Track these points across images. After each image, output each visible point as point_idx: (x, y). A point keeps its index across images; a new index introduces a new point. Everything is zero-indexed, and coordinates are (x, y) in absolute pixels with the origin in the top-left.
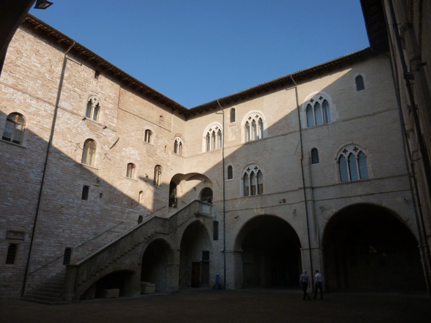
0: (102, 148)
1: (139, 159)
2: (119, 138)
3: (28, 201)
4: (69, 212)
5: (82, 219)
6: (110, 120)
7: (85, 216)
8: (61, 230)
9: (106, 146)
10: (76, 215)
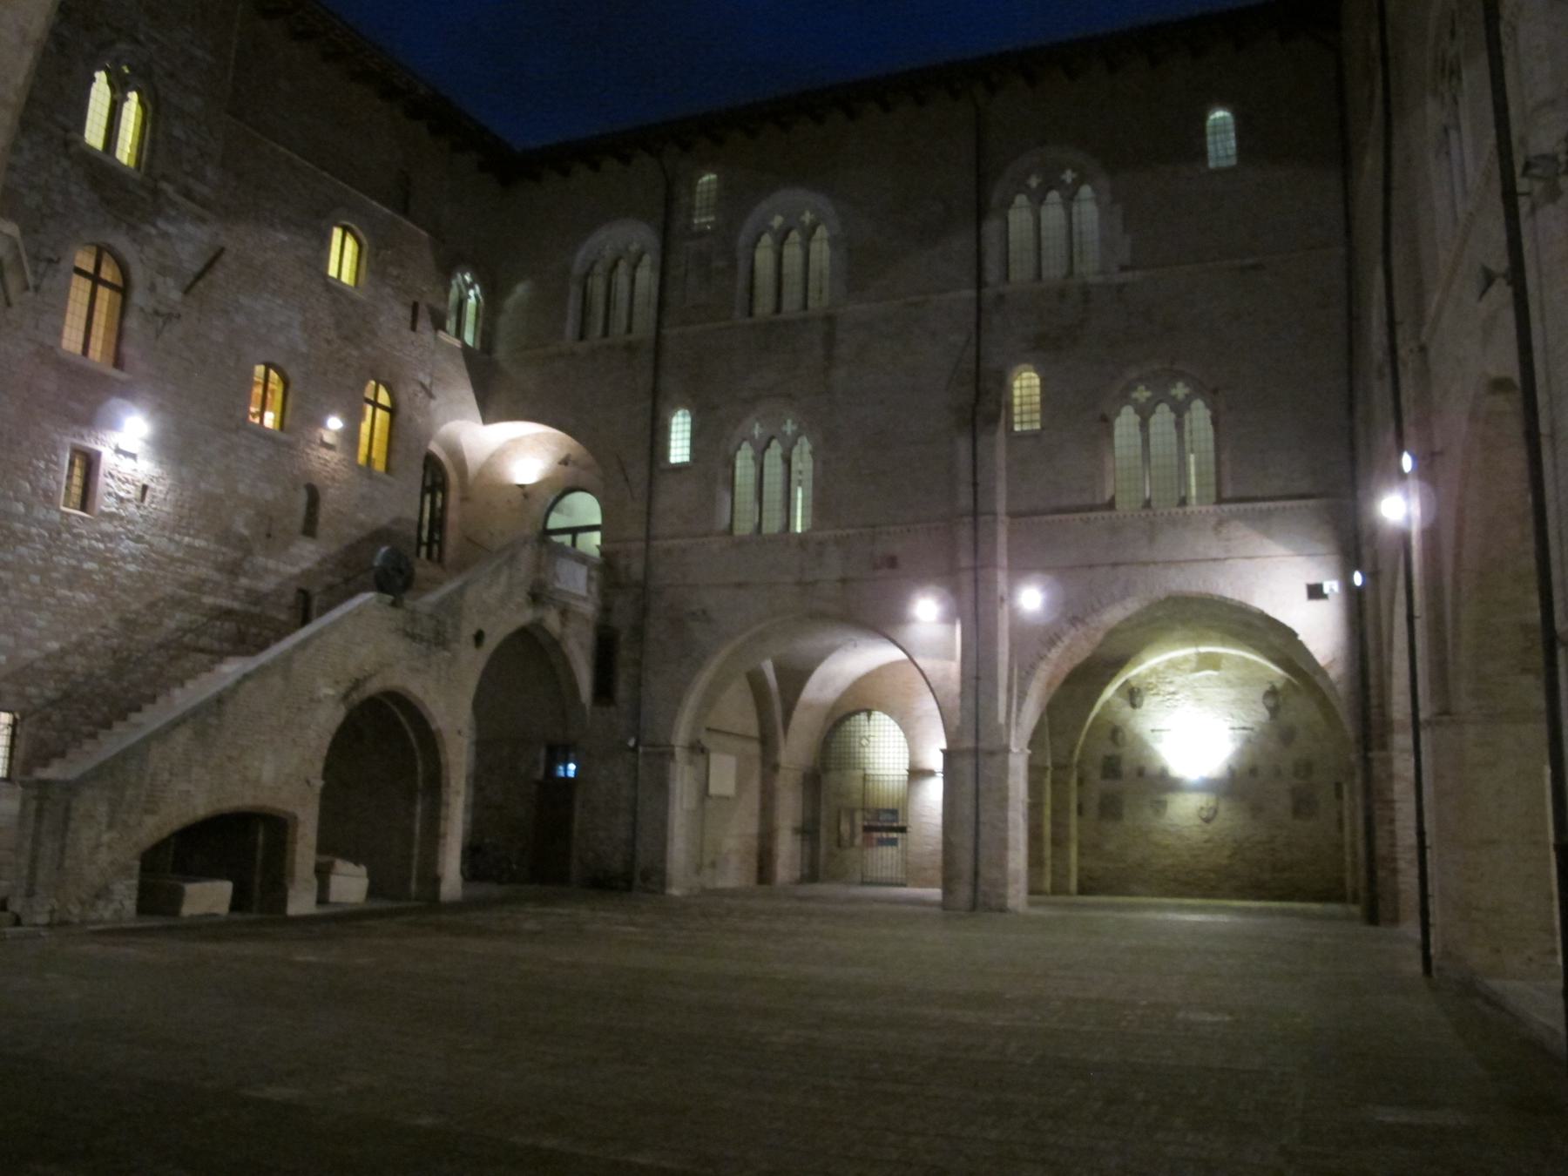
1: (304, 349)
2: (222, 250)
4: (10, 557)
6: (187, 168)
7: (75, 578)
9: (170, 282)
10: (37, 570)
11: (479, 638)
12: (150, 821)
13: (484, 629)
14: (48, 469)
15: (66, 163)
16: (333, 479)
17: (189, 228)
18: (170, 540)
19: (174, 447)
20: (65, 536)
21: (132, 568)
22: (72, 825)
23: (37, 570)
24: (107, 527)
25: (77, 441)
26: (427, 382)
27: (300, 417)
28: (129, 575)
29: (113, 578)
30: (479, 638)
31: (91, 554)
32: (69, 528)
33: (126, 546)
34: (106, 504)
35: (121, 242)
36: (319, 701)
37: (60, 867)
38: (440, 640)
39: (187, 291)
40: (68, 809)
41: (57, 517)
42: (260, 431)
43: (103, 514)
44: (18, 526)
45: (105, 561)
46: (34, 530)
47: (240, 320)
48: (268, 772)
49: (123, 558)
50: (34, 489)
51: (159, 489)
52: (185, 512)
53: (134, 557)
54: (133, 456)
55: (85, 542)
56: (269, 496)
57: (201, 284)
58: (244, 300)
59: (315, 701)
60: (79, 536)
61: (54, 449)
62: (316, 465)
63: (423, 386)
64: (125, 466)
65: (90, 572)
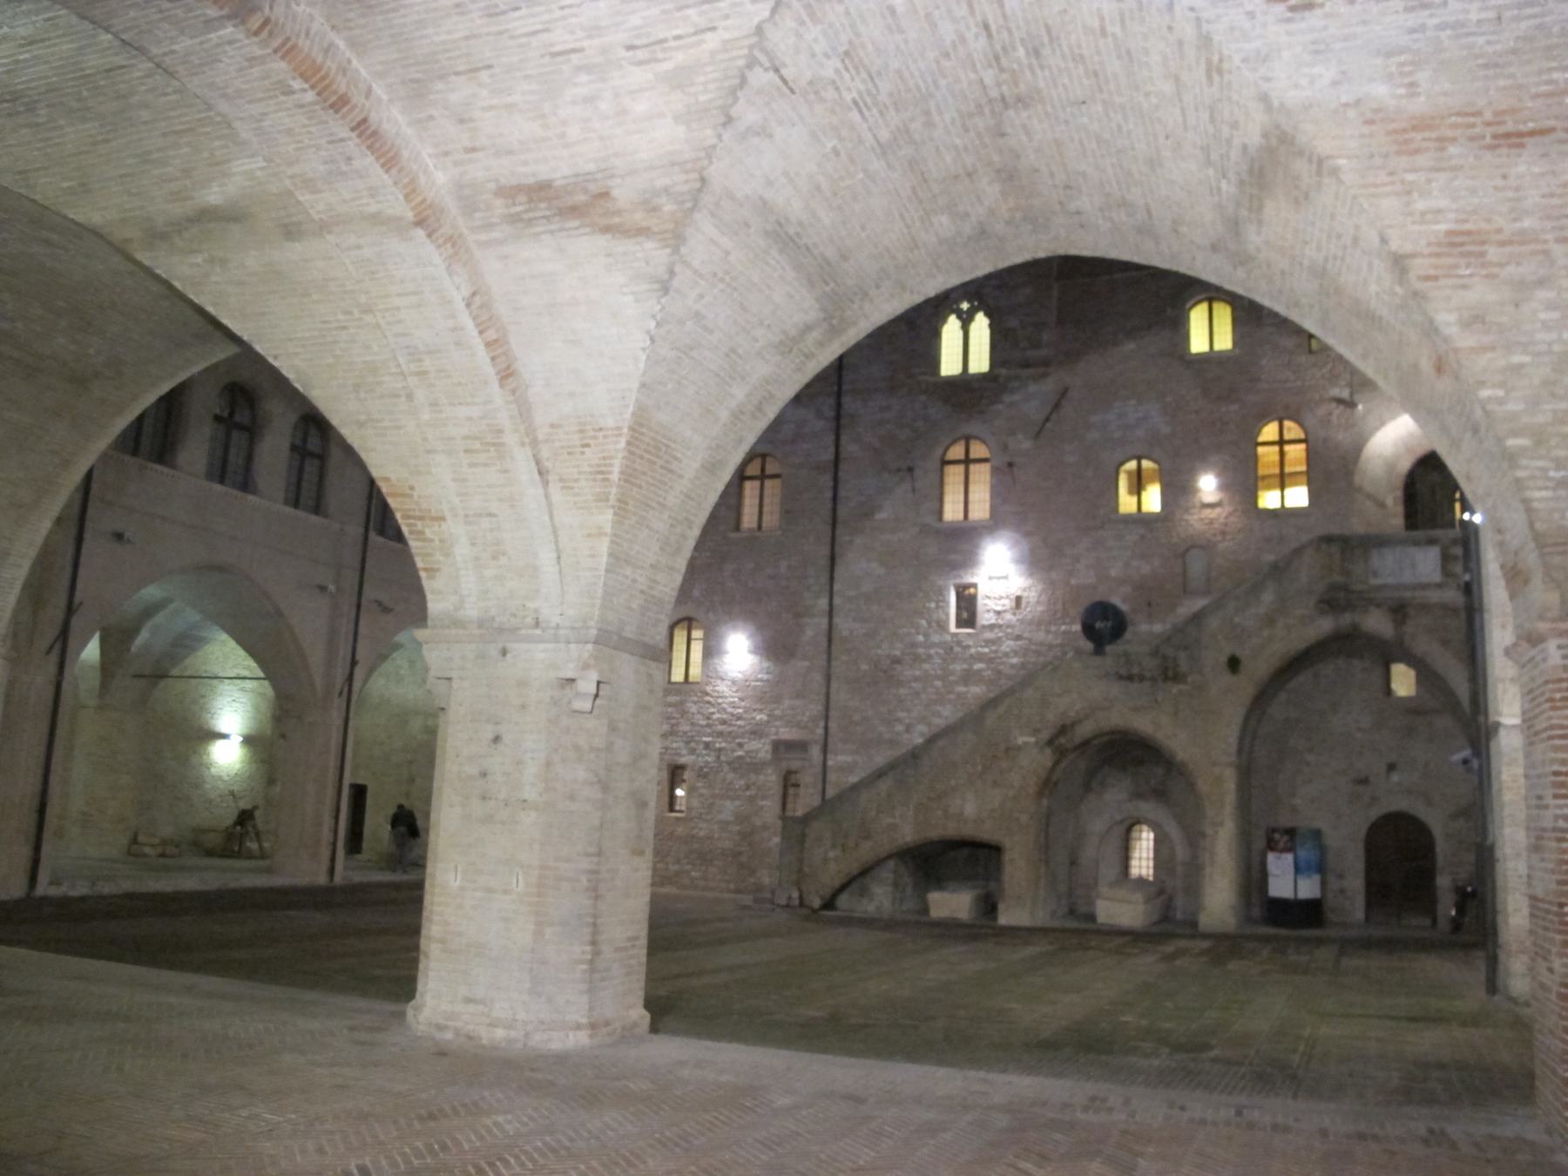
0: (1005, 447)
1: (1166, 430)
3: (806, 663)
4: (917, 673)
5: (962, 689)
7: (968, 677)
9: (1020, 436)
10: (937, 677)
11: (1234, 664)
12: (866, 846)
13: (1238, 653)
14: (938, 607)
15: (923, 398)
17: (1032, 388)
18: (1048, 632)
19: (1037, 561)
20: (957, 649)
21: (1015, 660)
22: (807, 845)
23: (937, 677)
24: (989, 635)
25: (958, 581)
26: (1345, 394)
27: (1178, 489)
28: (1013, 666)
29: (999, 672)
30: (1234, 664)
31: (980, 658)
32: (959, 643)
33: (1008, 645)
34: (985, 618)
35: (973, 428)
36: (1019, 748)
37: (800, 871)
38: (1170, 674)
40: (804, 835)
41: (948, 638)
42: (1141, 520)
43: (984, 627)
44: (921, 651)
45: (990, 661)
46: (932, 651)
47: (1094, 435)
48: (970, 809)
49: (1006, 655)
50: (929, 623)
51: (1032, 596)
52: (1059, 606)
53: (1016, 653)
54: (1006, 578)
55: (973, 651)
56: (1146, 569)
57: (1049, 425)
59: (1011, 751)
60: (968, 647)
62: (1199, 526)
63: (1340, 401)
65: (980, 671)
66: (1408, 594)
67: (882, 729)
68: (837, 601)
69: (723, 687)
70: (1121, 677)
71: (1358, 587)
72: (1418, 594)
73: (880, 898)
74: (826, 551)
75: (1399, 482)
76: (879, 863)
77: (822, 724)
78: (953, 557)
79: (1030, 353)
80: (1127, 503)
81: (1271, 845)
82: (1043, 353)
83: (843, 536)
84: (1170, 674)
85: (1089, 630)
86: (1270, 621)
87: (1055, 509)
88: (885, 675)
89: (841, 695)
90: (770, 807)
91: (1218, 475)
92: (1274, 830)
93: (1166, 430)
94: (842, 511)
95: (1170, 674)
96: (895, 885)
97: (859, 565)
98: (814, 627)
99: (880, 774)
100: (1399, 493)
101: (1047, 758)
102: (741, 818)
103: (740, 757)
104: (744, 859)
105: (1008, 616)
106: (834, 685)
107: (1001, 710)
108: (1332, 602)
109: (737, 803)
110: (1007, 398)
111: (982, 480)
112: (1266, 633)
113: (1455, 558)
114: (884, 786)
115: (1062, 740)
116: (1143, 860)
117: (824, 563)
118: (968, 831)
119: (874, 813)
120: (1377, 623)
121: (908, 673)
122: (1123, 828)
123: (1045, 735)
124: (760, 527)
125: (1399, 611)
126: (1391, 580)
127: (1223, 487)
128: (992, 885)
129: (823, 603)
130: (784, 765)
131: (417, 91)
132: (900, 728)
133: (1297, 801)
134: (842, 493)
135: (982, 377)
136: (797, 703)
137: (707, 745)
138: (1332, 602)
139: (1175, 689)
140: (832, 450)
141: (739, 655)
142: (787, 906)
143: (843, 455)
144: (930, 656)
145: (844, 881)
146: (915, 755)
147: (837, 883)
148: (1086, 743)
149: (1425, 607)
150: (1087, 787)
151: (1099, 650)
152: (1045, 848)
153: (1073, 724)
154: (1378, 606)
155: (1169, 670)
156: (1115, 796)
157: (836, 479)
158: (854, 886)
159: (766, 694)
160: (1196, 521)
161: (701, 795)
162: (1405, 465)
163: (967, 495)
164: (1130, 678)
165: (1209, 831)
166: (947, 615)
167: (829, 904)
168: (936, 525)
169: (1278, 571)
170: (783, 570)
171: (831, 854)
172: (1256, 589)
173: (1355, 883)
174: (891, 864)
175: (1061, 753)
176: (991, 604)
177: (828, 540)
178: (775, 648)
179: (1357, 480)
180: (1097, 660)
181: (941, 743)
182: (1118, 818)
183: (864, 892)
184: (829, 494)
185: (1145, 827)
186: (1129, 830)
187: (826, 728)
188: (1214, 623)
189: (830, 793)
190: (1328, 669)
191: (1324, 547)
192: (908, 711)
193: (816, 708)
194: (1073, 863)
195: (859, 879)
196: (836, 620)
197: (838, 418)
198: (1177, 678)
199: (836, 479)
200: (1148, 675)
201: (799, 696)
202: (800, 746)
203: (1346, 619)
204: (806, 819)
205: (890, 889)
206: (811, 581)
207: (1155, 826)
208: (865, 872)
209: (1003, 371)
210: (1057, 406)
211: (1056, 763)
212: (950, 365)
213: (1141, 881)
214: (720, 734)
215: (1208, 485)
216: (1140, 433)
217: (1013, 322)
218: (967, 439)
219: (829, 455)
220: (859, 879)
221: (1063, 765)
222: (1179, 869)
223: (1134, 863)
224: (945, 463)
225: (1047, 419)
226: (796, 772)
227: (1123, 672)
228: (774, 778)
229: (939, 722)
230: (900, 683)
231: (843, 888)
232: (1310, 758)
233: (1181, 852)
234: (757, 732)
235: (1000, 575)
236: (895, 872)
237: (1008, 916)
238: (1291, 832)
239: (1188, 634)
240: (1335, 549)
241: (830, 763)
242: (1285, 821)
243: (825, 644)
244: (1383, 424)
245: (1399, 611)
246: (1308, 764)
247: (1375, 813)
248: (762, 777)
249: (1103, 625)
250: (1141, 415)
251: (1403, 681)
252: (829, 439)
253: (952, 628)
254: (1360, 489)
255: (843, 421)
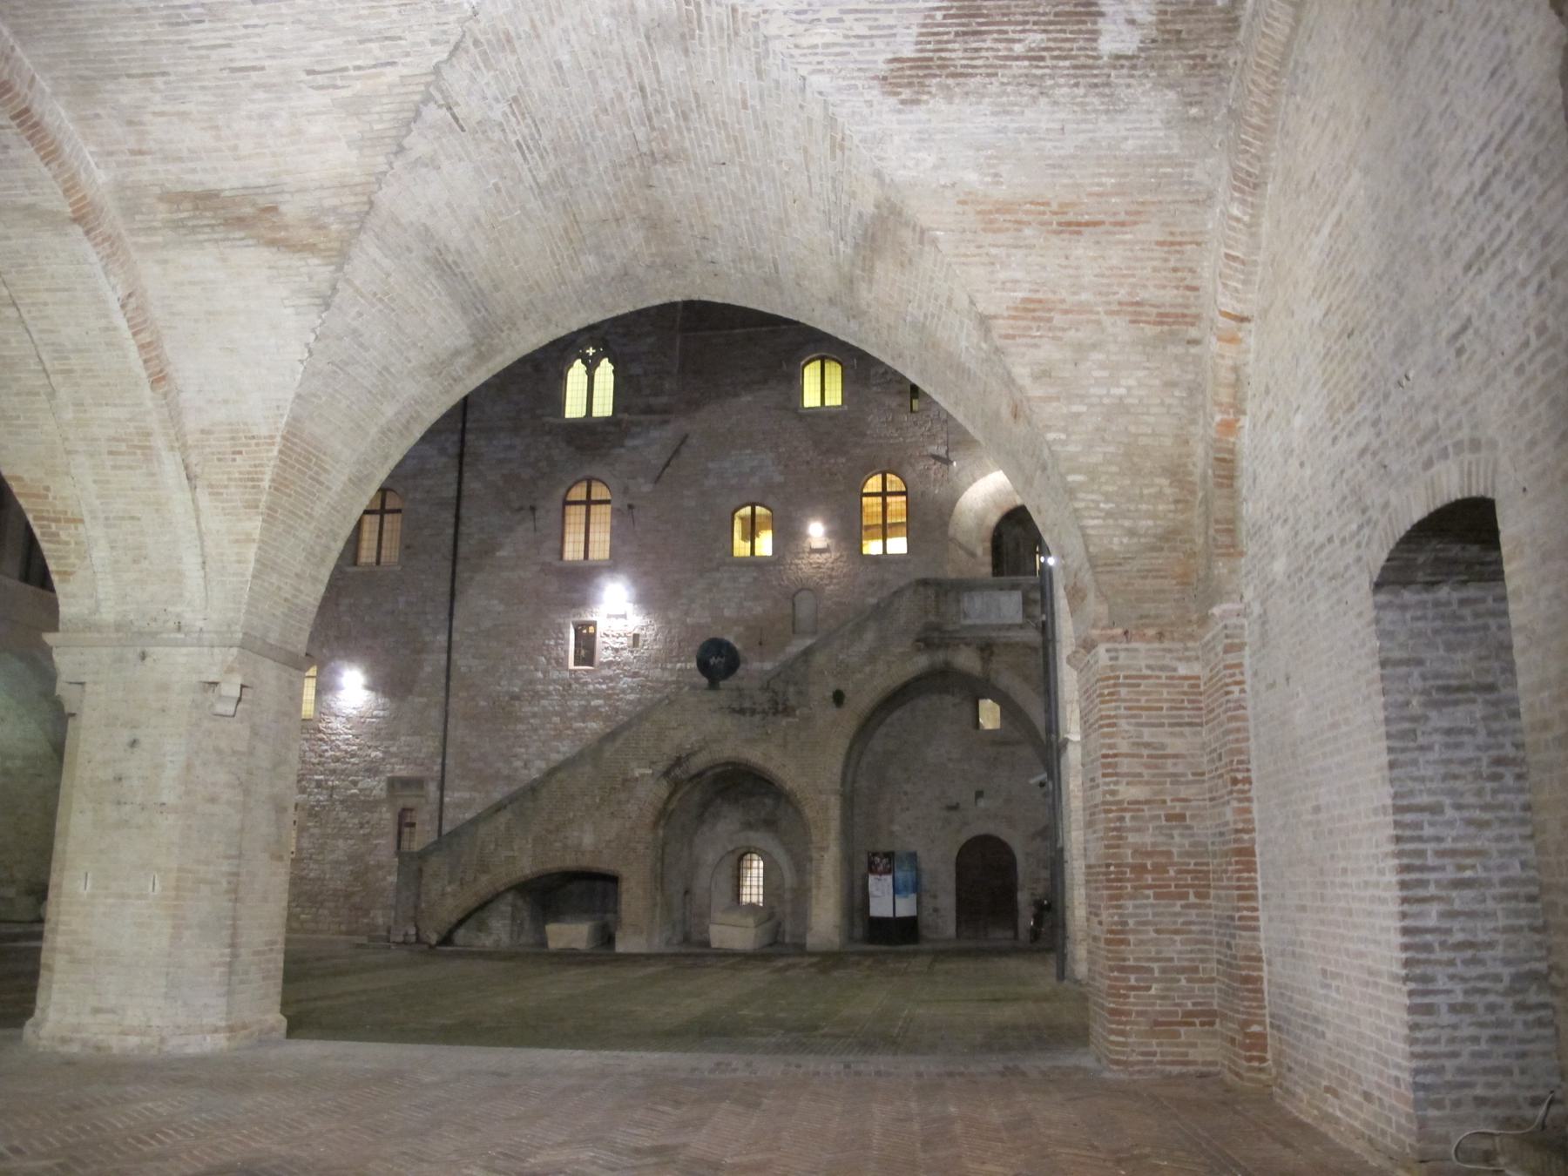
0: (626, 491)
1: (778, 479)
2: (686, 436)
3: (424, 700)
7: (586, 713)
8: (519, 764)
9: (641, 480)
10: (557, 714)
11: (838, 698)
12: (484, 879)
13: (842, 688)
14: (557, 644)
15: (547, 439)
16: (831, 577)
17: (654, 434)
18: (663, 669)
21: (631, 697)
23: (557, 714)
24: (607, 672)
26: (942, 452)
27: (788, 535)
28: (630, 702)
29: (617, 708)
30: (838, 698)
31: (598, 694)
32: (577, 680)
33: (624, 683)
34: (603, 655)
35: (595, 470)
36: (637, 779)
37: (416, 907)
38: (780, 708)
39: (657, 479)
40: (420, 870)
42: (754, 562)
44: (539, 687)
45: (609, 697)
48: (588, 840)
49: (623, 691)
51: (649, 634)
52: (675, 644)
53: (633, 690)
54: (624, 616)
56: (758, 610)
57: (668, 470)
58: (711, 465)
59: (628, 783)
60: (586, 683)
61: (560, 631)
63: (936, 458)
64: (618, 626)
66: (994, 634)
67: (500, 765)
68: (456, 637)
69: (336, 724)
70: (734, 711)
71: (950, 627)
72: (1002, 634)
73: (499, 931)
74: (446, 588)
75: (988, 534)
76: (497, 896)
77: (439, 760)
78: (576, 596)
79: (652, 400)
80: (741, 548)
81: (872, 868)
82: (664, 400)
83: (463, 574)
84: (780, 707)
85: (703, 666)
86: (871, 658)
87: (672, 555)
88: (503, 712)
89: (458, 732)
90: (384, 848)
91: (826, 522)
92: (874, 854)
93: (778, 479)
94: (463, 549)
95: (780, 707)
96: (513, 918)
97: (481, 603)
98: (433, 663)
99: (498, 808)
100: (988, 545)
101: (663, 790)
102: (354, 858)
103: (353, 795)
104: (357, 899)
105: (626, 654)
106: (451, 721)
107: (619, 743)
108: (929, 640)
109: (351, 842)
110: (629, 443)
111: (602, 517)
112: (867, 669)
113: (1035, 602)
114: (503, 818)
115: (678, 771)
116: (753, 888)
117: (446, 599)
118: (587, 862)
119: (492, 847)
120: (966, 660)
121: (527, 709)
122: (734, 858)
123: (661, 767)
124: (378, 562)
125: (987, 649)
126: (978, 622)
127: (830, 534)
128: (609, 917)
129: (442, 638)
130: (401, 803)
131: (84, 89)
132: (519, 764)
133: (896, 828)
134: (462, 528)
135: (605, 421)
136: (417, 738)
137: (319, 784)
138: (929, 640)
139: (784, 722)
140: (455, 486)
141: (354, 691)
142: (404, 943)
143: (465, 492)
144: (549, 693)
145: (461, 916)
146: (533, 789)
147: (454, 920)
148: (700, 775)
149: (1009, 645)
150: (701, 819)
151: (713, 685)
152: (660, 879)
153: (688, 756)
154: (968, 644)
155: (778, 703)
156: (726, 828)
157: (457, 517)
158: (471, 922)
159: (380, 731)
160: (806, 566)
161: (312, 835)
162: (993, 518)
163: (588, 535)
164: (742, 711)
165: (815, 855)
166: (566, 652)
167: (447, 940)
168: (558, 564)
169: (880, 612)
170: (401, 606)
171: (449, 889)
172: (859, 629)
173: (947, 902)
174: (510, 897)
175: (676, 786)
176: (610, 642)
177: (449, 576)
178: (390, 683)
179: (951, 532)
180: (712, 695)
181: (561, 775)
182: (730, 848)
183: (482, 927)
184: (451, 531)
185: (755, 856)
186: (741, 859)
187: (443, 765)
188: (820, 659)
189: (446, 828)
190: (922, 703)
191: (921, 589)
192: (527, 747)
193: (431, 745)
194: (687, 892)
195: (476, 914)
196: (455, 656)
197: (461, 456)
198: (787, 711)
199: (457, 517)
200: (759, 708)
201: (416, 732)
202: (415, 783)
203: (940, 656)
204: (423, 855)
205: (508, 922)
206: (429, 617)
207: (764, 855)
208: (483, 906)
209: (626, 416)
210: (677, 452)
211: (671, 795)
212: (574, 408)
213: (752, 906)
214: (334, 772)
215: (817, 532)
216: (755, 480)
217: (636, 369)
218: (589, 481)
219: (451, 492)
220: (476, 914)
221: (679, 796)
222: (788, 896)
223: (746, 891)
224: (566, 503)
225: (667, 465)
226: (411, 810)
227: (736, 705)
228: (388, 816)
229: (556, 758)
230: (520, 720)
231: (461, 922)
232: (908, 787)
233: (789, 879)
234: (372, 770)
235: (617, 613)
236: (514, 906)
237: (625, 944)
238: (890, 856)
239: (796, 671)
240: (931, 592)
241: (446, 799)
242: (883, 847)
243: (443, 681)
244: (975, 480)
245: (987, 649)
246: (906, 793)
247: (964, 837)
248: (376, 815)
249: (717, 661)
250: (755, 463)
251: (990, 715)
252: (452, 476)
253: (571, 666)
254: (952, 540)
255: (467, 459)
